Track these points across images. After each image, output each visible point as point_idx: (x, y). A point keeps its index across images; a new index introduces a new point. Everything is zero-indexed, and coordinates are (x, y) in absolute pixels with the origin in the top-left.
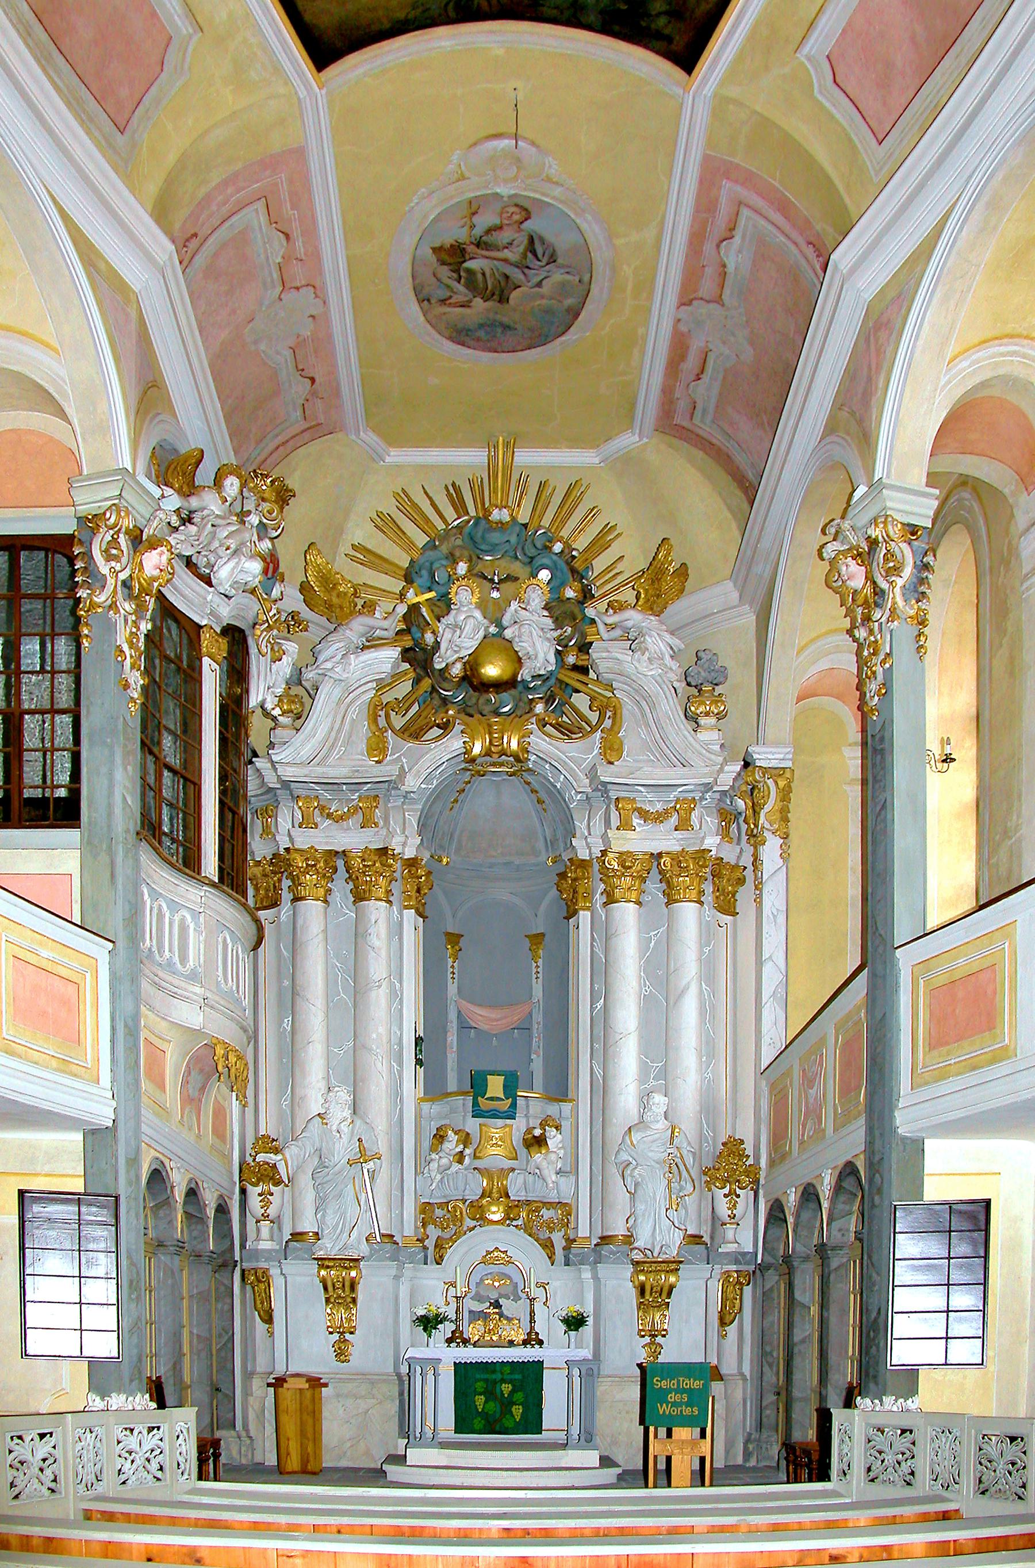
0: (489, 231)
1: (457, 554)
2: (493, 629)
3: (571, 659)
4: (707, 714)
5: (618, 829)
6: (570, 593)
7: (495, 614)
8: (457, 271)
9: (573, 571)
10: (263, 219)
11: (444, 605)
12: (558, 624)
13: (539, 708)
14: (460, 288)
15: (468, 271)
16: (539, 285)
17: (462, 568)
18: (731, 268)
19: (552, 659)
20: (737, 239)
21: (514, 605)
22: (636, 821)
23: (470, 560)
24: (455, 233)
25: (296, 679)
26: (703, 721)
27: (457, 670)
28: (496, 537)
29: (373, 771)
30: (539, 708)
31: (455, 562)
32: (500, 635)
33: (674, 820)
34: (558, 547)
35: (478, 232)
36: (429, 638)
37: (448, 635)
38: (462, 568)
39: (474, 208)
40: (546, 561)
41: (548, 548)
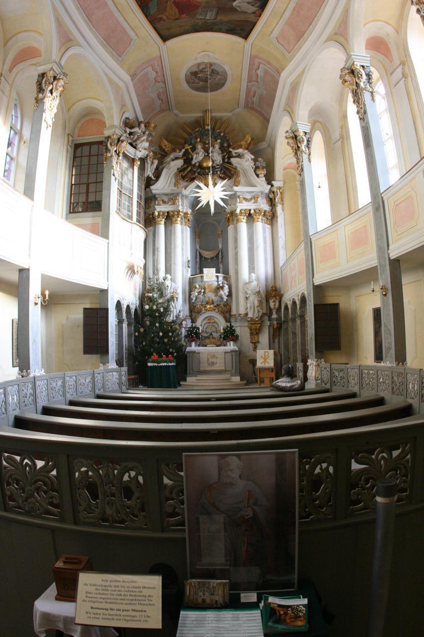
0: (203, 69)
1: (197, 136)
2: (206, 154)
3: (226, 161)
4: (261, 174)
6: (225, 145)
7: (206, 150)
8: (196, 77)
10: (151, 70)
11: (194, 149)
12: (223, 152)
13: (219, 173)
14: (197, 80)
15: (199, 77)
16: (215, 79)
17: (199, 140)
18: (259, 75)
19: (221, 161)
20: (260, 70)
22: (244, 201)
23: (200, 138)
24: (195, 69)
25: (157, 169)
26: (260, 175)
27: (197, 164)
29: (175, 190)
30: (219, 173)
31: (196, 138)
33: (253, 201)
34: (222, 134)
35: (200, 69)
36: (190, 157)
37: (195, 156)
38: (199, 140)
39: (199, 65)
41: (220, 135)
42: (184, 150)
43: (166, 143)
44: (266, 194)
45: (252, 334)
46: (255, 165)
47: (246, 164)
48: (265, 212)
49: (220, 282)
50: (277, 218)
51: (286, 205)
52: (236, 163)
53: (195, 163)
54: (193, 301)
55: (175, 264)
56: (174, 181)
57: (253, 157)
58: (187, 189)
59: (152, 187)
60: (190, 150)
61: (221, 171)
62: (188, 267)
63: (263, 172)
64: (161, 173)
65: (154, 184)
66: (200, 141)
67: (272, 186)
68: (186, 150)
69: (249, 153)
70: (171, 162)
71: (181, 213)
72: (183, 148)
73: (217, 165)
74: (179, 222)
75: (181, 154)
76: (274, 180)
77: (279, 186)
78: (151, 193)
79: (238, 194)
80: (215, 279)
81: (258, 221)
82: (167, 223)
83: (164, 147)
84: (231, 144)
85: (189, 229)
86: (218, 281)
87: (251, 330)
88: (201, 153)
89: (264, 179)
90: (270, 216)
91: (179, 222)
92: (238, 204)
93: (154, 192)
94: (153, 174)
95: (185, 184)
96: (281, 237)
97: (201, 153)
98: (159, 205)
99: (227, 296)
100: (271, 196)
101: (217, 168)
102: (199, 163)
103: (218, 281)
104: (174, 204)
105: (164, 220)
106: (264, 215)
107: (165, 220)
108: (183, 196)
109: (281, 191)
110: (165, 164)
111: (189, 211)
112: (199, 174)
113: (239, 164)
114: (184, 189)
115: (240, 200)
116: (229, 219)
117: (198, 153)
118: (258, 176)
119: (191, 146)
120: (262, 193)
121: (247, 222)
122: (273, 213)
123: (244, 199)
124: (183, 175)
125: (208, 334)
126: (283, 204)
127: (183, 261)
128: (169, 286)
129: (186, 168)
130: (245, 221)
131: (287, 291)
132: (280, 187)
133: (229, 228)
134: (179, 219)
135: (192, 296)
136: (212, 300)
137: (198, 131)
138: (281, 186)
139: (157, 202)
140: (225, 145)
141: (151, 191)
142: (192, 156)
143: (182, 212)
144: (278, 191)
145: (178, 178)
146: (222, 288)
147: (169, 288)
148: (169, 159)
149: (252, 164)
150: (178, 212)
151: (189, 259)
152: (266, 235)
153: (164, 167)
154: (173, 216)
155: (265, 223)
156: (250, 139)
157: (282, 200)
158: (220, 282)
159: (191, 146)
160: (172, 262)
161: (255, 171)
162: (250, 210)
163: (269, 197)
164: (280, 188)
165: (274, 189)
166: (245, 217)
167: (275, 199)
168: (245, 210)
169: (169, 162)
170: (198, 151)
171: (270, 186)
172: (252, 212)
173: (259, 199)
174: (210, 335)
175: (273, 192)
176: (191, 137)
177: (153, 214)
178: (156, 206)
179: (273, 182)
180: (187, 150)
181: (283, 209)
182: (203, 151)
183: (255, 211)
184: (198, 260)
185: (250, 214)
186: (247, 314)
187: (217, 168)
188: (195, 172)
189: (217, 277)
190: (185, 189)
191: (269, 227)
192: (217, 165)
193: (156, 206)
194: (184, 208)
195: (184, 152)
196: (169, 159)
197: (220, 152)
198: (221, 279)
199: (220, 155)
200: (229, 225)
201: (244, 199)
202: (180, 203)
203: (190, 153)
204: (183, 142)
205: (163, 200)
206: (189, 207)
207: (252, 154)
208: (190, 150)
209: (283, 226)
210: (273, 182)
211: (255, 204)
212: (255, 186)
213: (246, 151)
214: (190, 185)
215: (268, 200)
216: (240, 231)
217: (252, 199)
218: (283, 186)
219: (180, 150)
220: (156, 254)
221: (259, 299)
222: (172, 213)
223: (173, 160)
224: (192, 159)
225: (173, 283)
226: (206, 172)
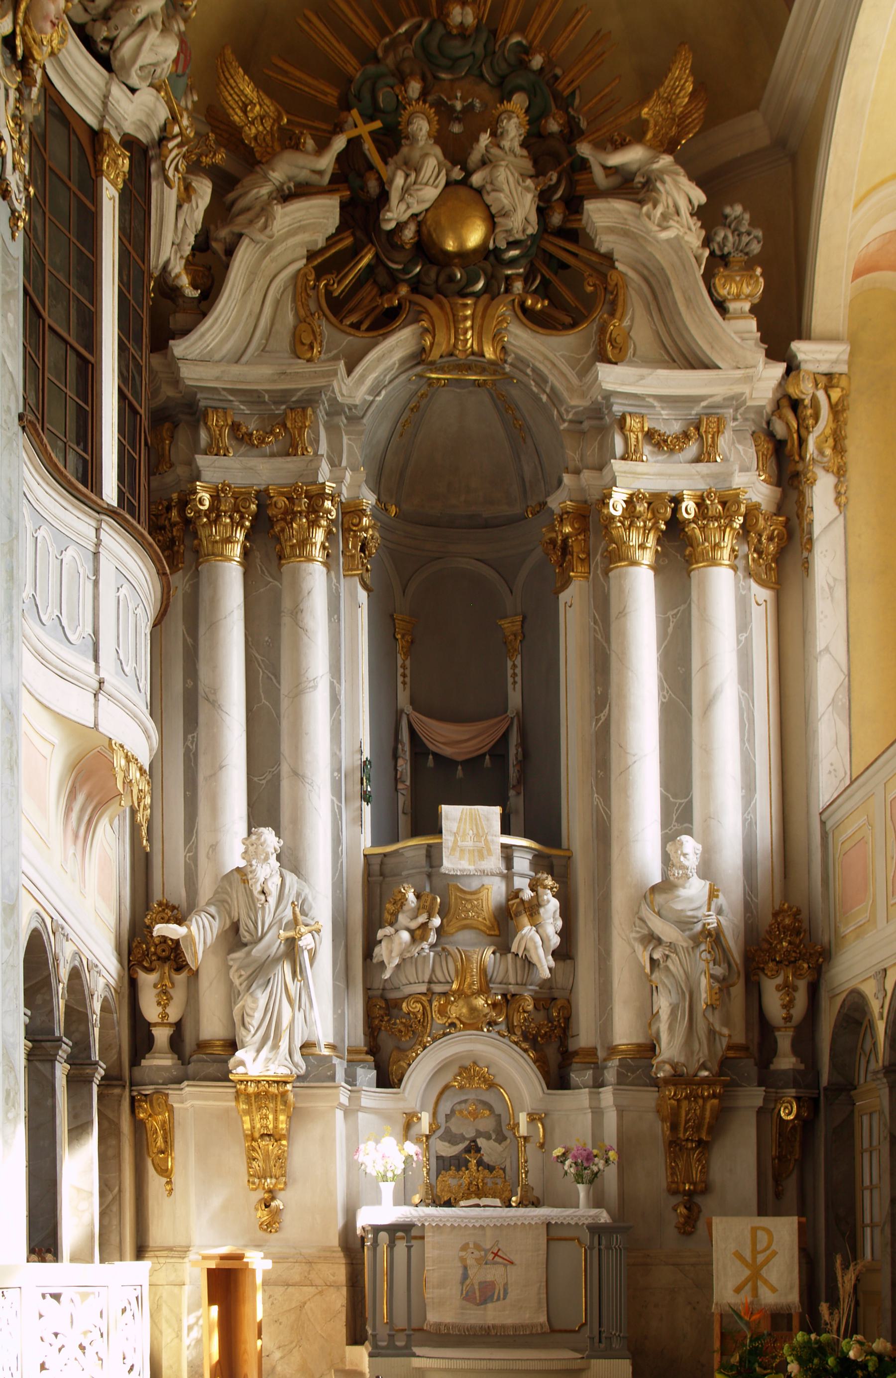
1: (406, 68)
2: (457, 174)
3: (556, 219)
4: (737, 298)
5: (623, 458)
6: (553, 126)
9: (556, 96)
12: (539, 172)
13: (518, 286)
17: (415, 88)
19: (534, 218)
21: (485, 139)
22: (647, 449)
23: (424, 79)
25: (202, 244)
27: (409, 233)
28: (456, 48)
30: (518, 286)
31: (403, 81)
32: (465, 182)
33: (692, 448)
34: (537, 61)
36: (372, 186)
38: (415, 88)
40: (520, 81)
41: (523, 65)
42: (339, 143)
43: (249, 90)
44: (759, 410)
45: (674, 1146)
46: (707, 242)
47: (664, 235)
48: (752, 512)
49: (521, 883)
50: (810, 543)
51: (854, 474)
52: (611, 230)
53: (400, 226)
54: (387, 975)
55: (297, 775)
56: (290, 318)
57: (699, 197)
58: (359, 370)
59: (179, 348)
60: (369, 146)
61: (527, 279)
62: (366, 797)
63: (747, 290)
64: (226, 267)
65: (185, 332)
66: (424, 95)
67: (792, 368)
68: (350, 141)
69: (681, 171)
70: (279, 210)
71: (328, 504)
72: (338, 129)
73: (512, 245)
74: (317, 553)
75: (326, 162)
76: (801, 332)
77: (824, 368)
78: (176, 381)
79: (617, 409)
80: (495, 862)
81: (714, 562)
82: (257, 555)
83: (237, 117)
84: (583, 124)
85: (363, 596)
86: (508, 877)
87: (674, 1127)
88: (431, 165)
89: (753, 324)
90: (771, 539)
91: (317, 553)
92: (617, 465)
93: (190, 374)
94: (189, 264)
95: (347, 341)
96: (827, 649)
97: (431, 165)
98: (214, 449)
99: (555, 954)
100: (779, 429)
101: (512, 262)
102: (419, 225)
103: (508, 877)
104: (291, 448)
105: (240, 535)
106: (745, 530)
107: (247, 537)
108: (336, 409)
109: (835, 394)
110: (242, 219)
111: (369, 499)
112: (416, 286)
113: (626, 233)
114: (342, 365)
115: (626, 440)
116: (565, 549)
117: (413, 167)
118: (721, 306)
119: (377, 125)
120: (736, 401)
121: (657, 568)
122: (787, 524)
123: (650, 435)
124: (337, 290)
125: (462, 1146)
126: (840, 472)
127: (336, 767)
128: (273, 887)
129: (354, 252)
130: (647, 557)
131: (860, 932)
132: (829, 376)
133: (564, 597)
134: (319, 536)
135: (381, 952)
136: (483, 971)
137: (409, 34)
138: (837, 369)
139: (203, 435)
140: (553, 126)
141: (172, 364)
142: (380, 179)
143: (332, 498)
144: (821, 395)
145: (313, 307)
146: (533, 909)
147: (272, 900)
148: (265, 190)
149: (693, 237)
150: (317, 497)
151: (367, 754)
152: (749, 640)
153: (240, 236)
154: (290, 515)
155: (749, 574)
156: (690, 87)
157: (839, 448)
158: (521, 883)
159: (377, 125)
160: (285, 769)
161: (708, 277)
162: (677, 500)
163: (771, 435)
164: (830, 379)
165: (805, 389)
166: (651, 541)
167: (802, 442)
168: (654, 500)
169: (265, 211)
170: (416, 154)
171: (779, 369)
172: (688, 508)
173: (723, 442)
174: (468, 1150)
175: (795, 405)
176: (372, 69)
177: (186, 499)
178: (202, 460)
179: (801, 349)
180: (354, 144)
181: (840, 498)
182: (438, 151)
183: (700, 504)
184: (404, 765)
185: (675, 525)
186: (649, 1049)
187: (512, 262)
188: (394, 280)
189: (507, 852)
190: (349, 371)
191: (761, 594)
192: (512, 245)
193: (202, 460)
194: (339, 481)
195: (341, 158)
196: (265, 190)
197: (527, 165)
198: (522, 863)
199: (529, 182)
200: (566, 583)
201: (650, 435)
202: (323, 449)
203: (371, 167)
204: (331, 96)
205: (235, 427)
206: (366, 482)
207: (701, 183)
208: (369, 146)
209: (840, 592)
210: (801, 349)
211: (702, 467)
212: (707, 365)
213: (666, 160)
214: (376, 344)
215: (767, 446)
216: (623, 613)
217: (686, 435)
218: (844, 368)
219: (322, 146)
220: (202, 718)
221: (719, 971)
222: (282, 502)
223: (286, 196)
224: (384, 197)
225: (290, 877)
226: (451, 279)
